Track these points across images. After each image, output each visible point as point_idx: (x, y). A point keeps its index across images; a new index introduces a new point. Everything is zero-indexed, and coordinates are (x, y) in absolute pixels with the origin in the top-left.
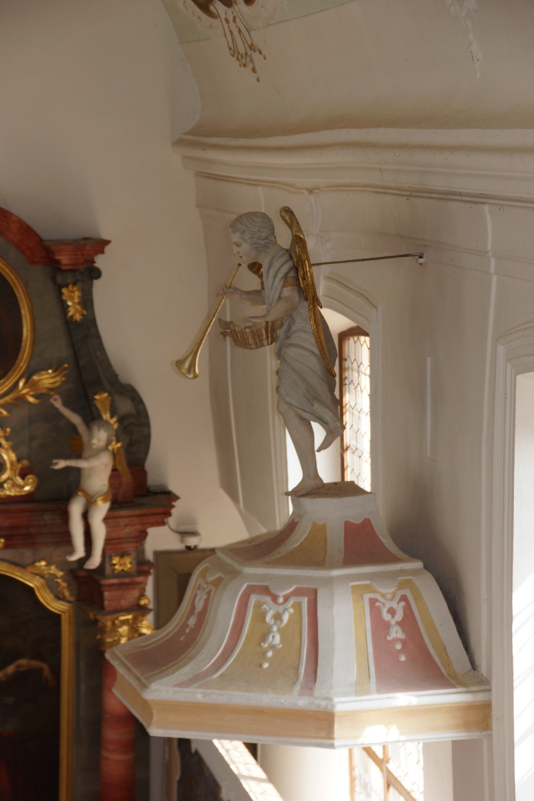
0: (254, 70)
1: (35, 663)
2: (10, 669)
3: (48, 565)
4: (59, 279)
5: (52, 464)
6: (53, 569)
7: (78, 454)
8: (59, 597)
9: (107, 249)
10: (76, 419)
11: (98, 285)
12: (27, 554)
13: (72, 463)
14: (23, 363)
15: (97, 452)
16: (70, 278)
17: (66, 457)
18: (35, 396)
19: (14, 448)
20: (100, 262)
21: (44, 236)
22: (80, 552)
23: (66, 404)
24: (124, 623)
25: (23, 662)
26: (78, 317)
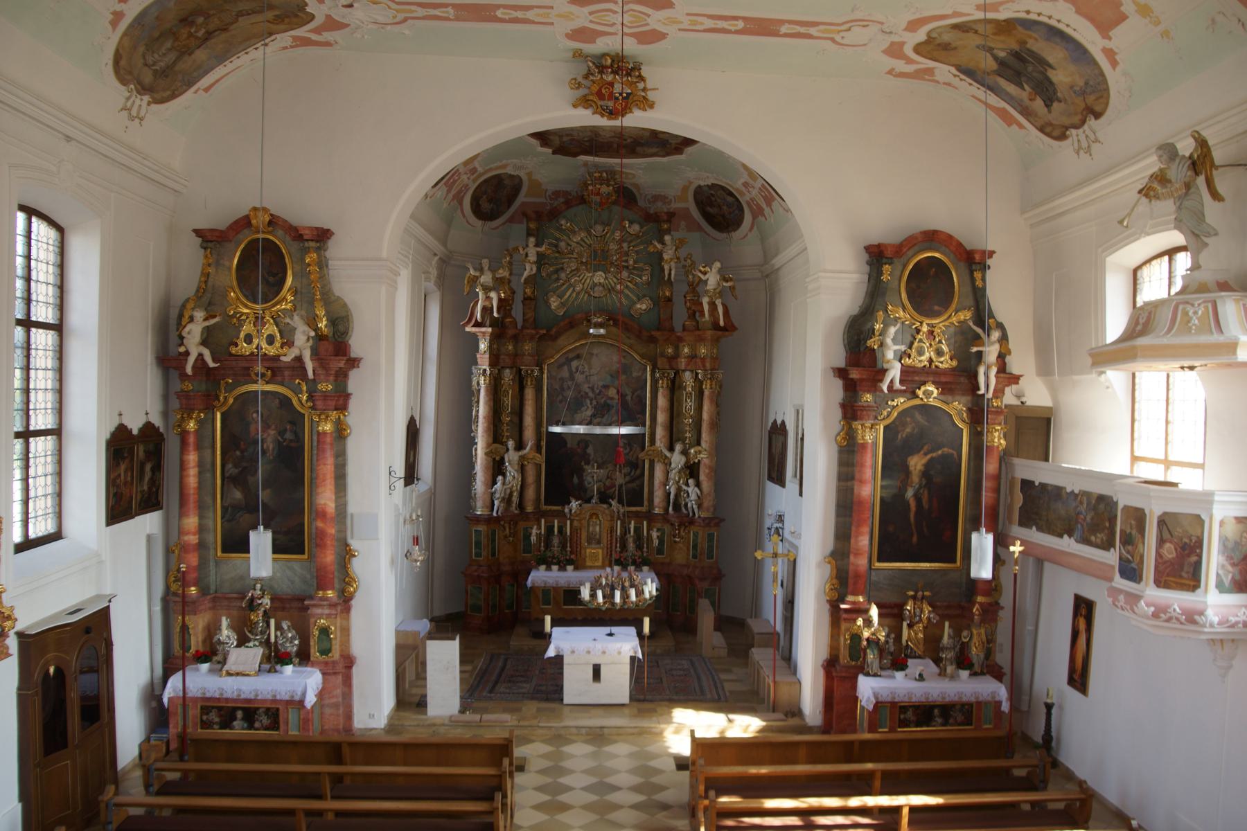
0: (1091, 155)
1: (951, 451)
2: (940, 452)
3: (959, 404)
4: (974, 267)
5: (970, 348)
6: (960, 407)
7: (983, 345)
8: (964, 421)
9: (994, 256)
10: (979, 331)
11: (988, 272)
12: (950, 398)
13: (980, 349)
14: (954, 305)
15: (993, 343)
16: (978, 267)
17: (977, 346)
18: (958, 322)
19: (948, 345)
20: (989, 262)
21: (968, 249)
22: (982, 391)
23: (974, 324)
24: (996, 430)
25: (945, 449)
26: (981, 286)
